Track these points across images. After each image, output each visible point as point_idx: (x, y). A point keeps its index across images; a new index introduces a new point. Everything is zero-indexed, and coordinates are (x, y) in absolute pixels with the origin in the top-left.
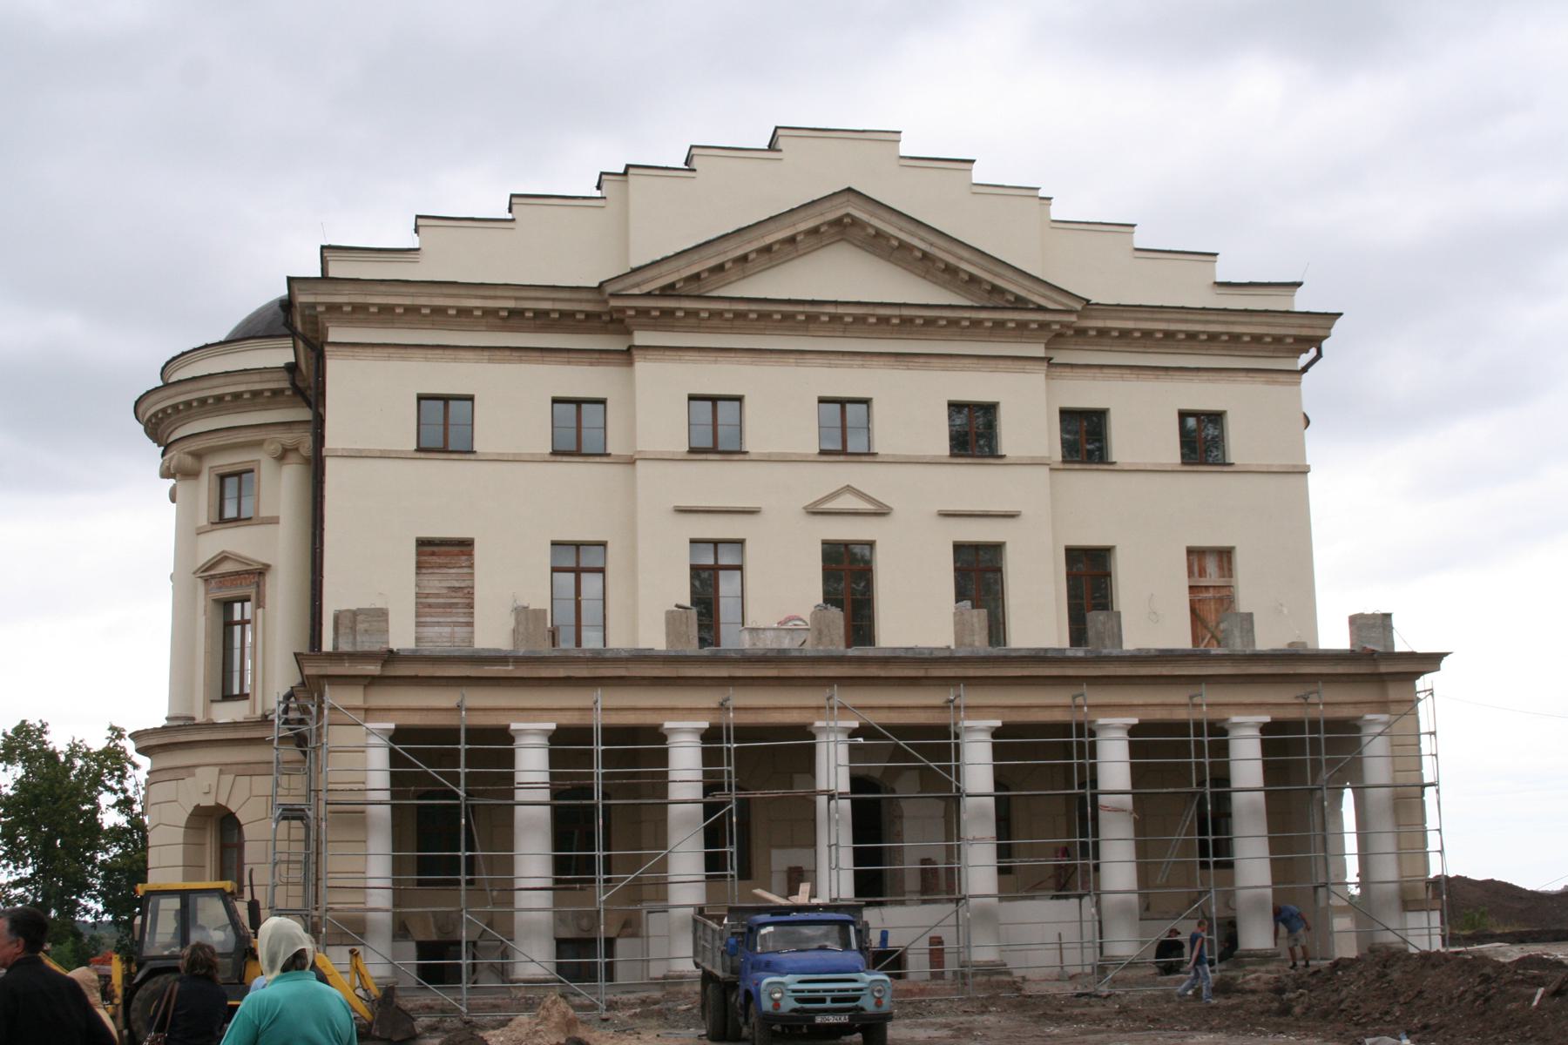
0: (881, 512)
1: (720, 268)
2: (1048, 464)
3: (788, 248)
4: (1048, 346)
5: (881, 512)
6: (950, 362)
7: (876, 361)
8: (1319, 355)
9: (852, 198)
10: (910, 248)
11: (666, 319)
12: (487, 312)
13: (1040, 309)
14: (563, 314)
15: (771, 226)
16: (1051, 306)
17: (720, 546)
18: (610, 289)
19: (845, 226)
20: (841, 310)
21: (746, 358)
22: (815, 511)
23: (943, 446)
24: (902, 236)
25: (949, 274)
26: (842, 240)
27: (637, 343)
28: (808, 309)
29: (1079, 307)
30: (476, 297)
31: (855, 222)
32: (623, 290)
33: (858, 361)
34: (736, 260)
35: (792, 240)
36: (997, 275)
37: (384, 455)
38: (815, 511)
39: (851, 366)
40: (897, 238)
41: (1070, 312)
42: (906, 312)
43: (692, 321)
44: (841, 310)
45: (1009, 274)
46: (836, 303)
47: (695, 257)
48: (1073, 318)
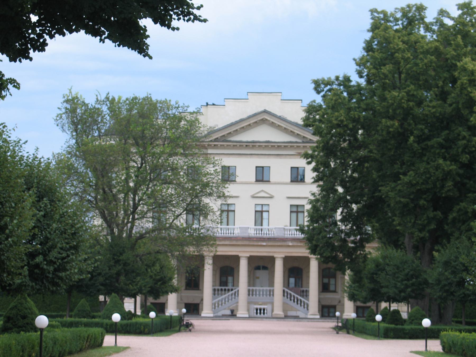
1: (230, 133)
5: (271, 197)
6: (291, 157)
7: (272, 157)
9: (265, 114)
10: (282, 127)
11: (215, 147)
20: (261, 144)
21: (237, 156)
23: (289, 180)
31: (266, 120)
33: (267, 157)
34: (234, 131)
35: (250, 125)
36: (304, 133)
38: (253, 197)
42: (279, 144)
44: (261, 144)
47: (223, 131)
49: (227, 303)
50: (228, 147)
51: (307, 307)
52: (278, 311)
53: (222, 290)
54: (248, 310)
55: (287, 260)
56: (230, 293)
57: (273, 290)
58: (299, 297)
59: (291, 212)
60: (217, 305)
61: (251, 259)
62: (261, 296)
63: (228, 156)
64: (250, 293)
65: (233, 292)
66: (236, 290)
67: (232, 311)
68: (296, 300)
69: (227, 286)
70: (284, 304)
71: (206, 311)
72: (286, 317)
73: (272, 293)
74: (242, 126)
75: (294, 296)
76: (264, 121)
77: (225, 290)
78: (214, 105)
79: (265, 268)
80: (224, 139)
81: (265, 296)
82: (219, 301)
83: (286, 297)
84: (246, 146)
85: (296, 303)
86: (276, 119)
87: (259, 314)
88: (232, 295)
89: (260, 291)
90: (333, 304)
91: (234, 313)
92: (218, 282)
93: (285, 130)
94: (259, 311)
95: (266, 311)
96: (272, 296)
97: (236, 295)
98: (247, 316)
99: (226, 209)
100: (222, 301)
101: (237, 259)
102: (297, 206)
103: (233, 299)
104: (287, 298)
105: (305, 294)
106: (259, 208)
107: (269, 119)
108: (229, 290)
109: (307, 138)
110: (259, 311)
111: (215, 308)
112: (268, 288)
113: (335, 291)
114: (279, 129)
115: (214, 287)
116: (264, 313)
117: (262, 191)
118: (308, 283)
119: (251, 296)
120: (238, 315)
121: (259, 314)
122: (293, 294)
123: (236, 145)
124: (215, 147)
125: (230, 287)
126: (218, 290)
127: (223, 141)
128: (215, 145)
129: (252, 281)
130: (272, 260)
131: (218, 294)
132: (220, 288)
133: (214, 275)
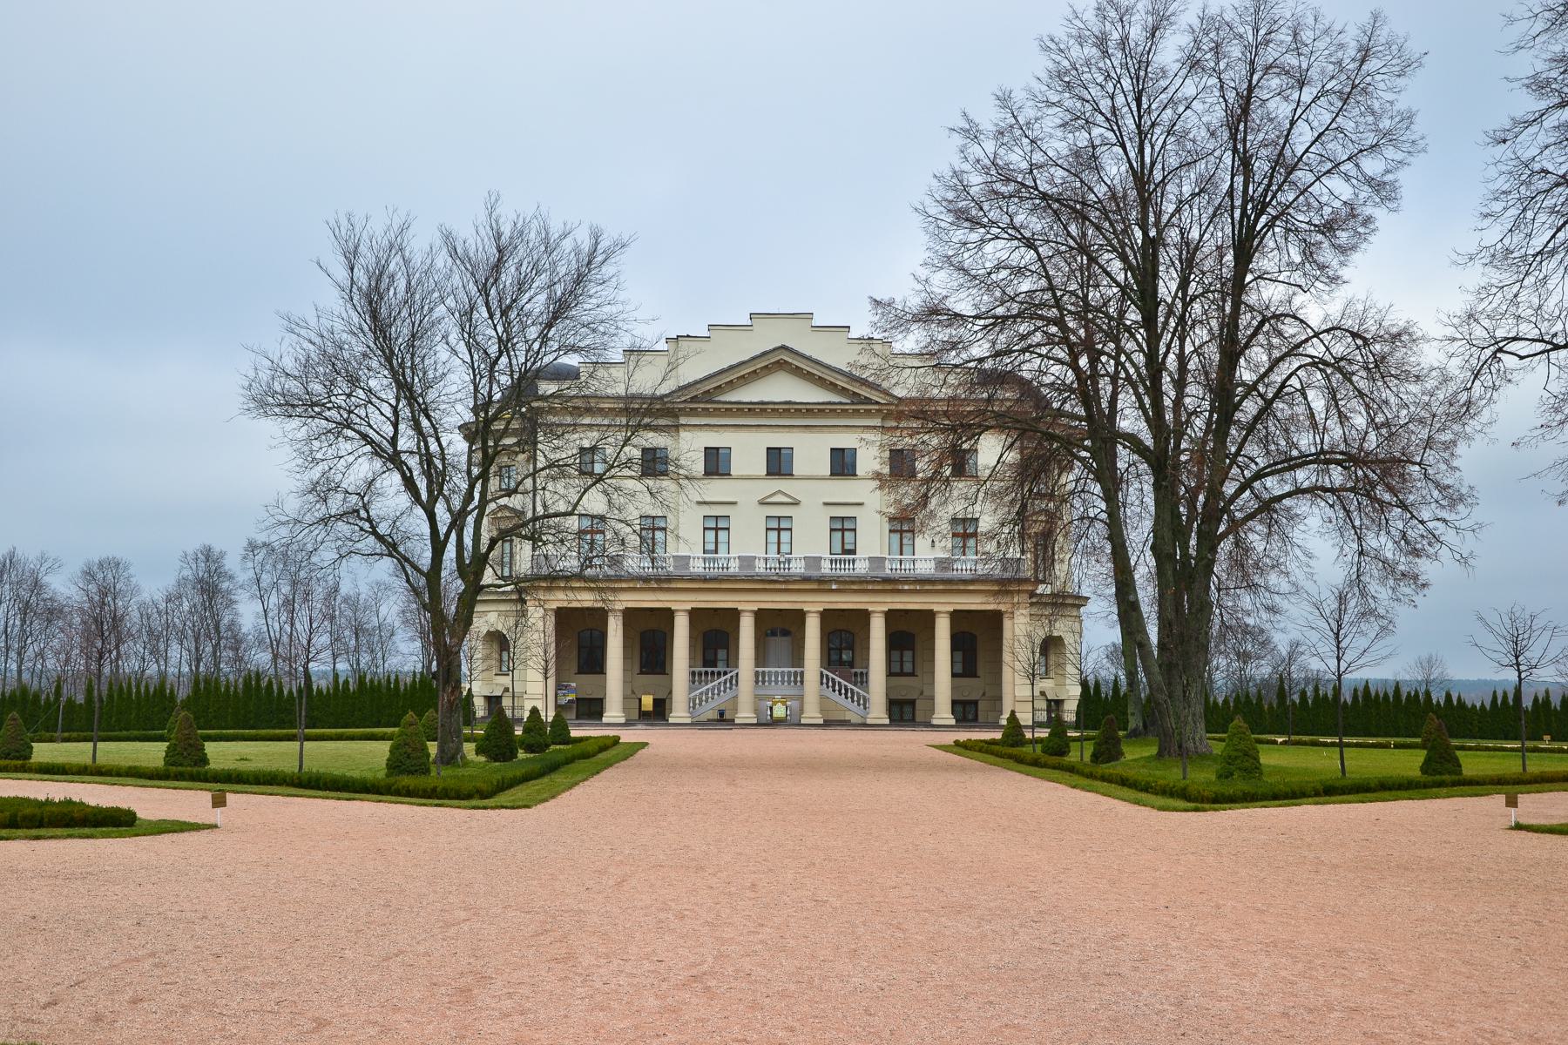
0: (796, 503)
3: (754, 375)
5: (796, 503)
6: (832, 429)
7: (795, 430)
11: (693, 412)
13: (877, 403)
15: (743, 366)
18: (666, 400)
22: (762, 503)
24: (808, 369)
28: (760, 406)
33: (787, 430)
38: (762, 503)
41: (892, 404)
42: (808, 407)
44: (776, 407)
46: (775, 403)
49: (716, 696)
50: (717, 413)
51: (865, 703)
52: (812, 714)
53: (706, 673)
55: (826, 616)
56: (723, 679)
57: (802, 674)
58: (850, 686)
59: (832, 530)
60: (697, 701)
61: (760, 616)
64: (759, 679)
65: (728, 676)
66: (734, 673)
68: (843, 691)
69: (716, 666)
70: (822, 697)
71: (679, 711)
72: (828, 724)
73: (799, 679)
74: (742, 373)
75: (840, 683)
76: (781, 366)
77: (713, 673)
78: (688, 336)
79: (785, 633)
80: (708, 396)
81: (786, 684)
82: (701, 693)
83: (825, 686)
84: (749, 409)
85: (843, 696)
86: (804, 361)
88: (725, 683)
89: (776, 673)
90: (973, 697)
91: (727, 716)
93: (821, 382)
96: (799, 684)
97: (734, 682)
98: (755, 721)
100: (707, 694)
101: (734, 615)
102: (843, 518)
103: (728, 690)
104: (828, 687)
105: (862, 679)
107: (790, 361)
108: (719, 673)
111: (694, 708)
112: (792, 670)
113: (913, 674)
118: (867, 659)
119: (760, 684)
120: (737, 721)
122: (837, 679)
123: (731, 409)
125: (722, 669)
126: (700, 674)
127: (707, 402)
129: (761, 658)
130: (800, 616)
131: (700, 683)
132: (703, 670)
133: (692, 646)
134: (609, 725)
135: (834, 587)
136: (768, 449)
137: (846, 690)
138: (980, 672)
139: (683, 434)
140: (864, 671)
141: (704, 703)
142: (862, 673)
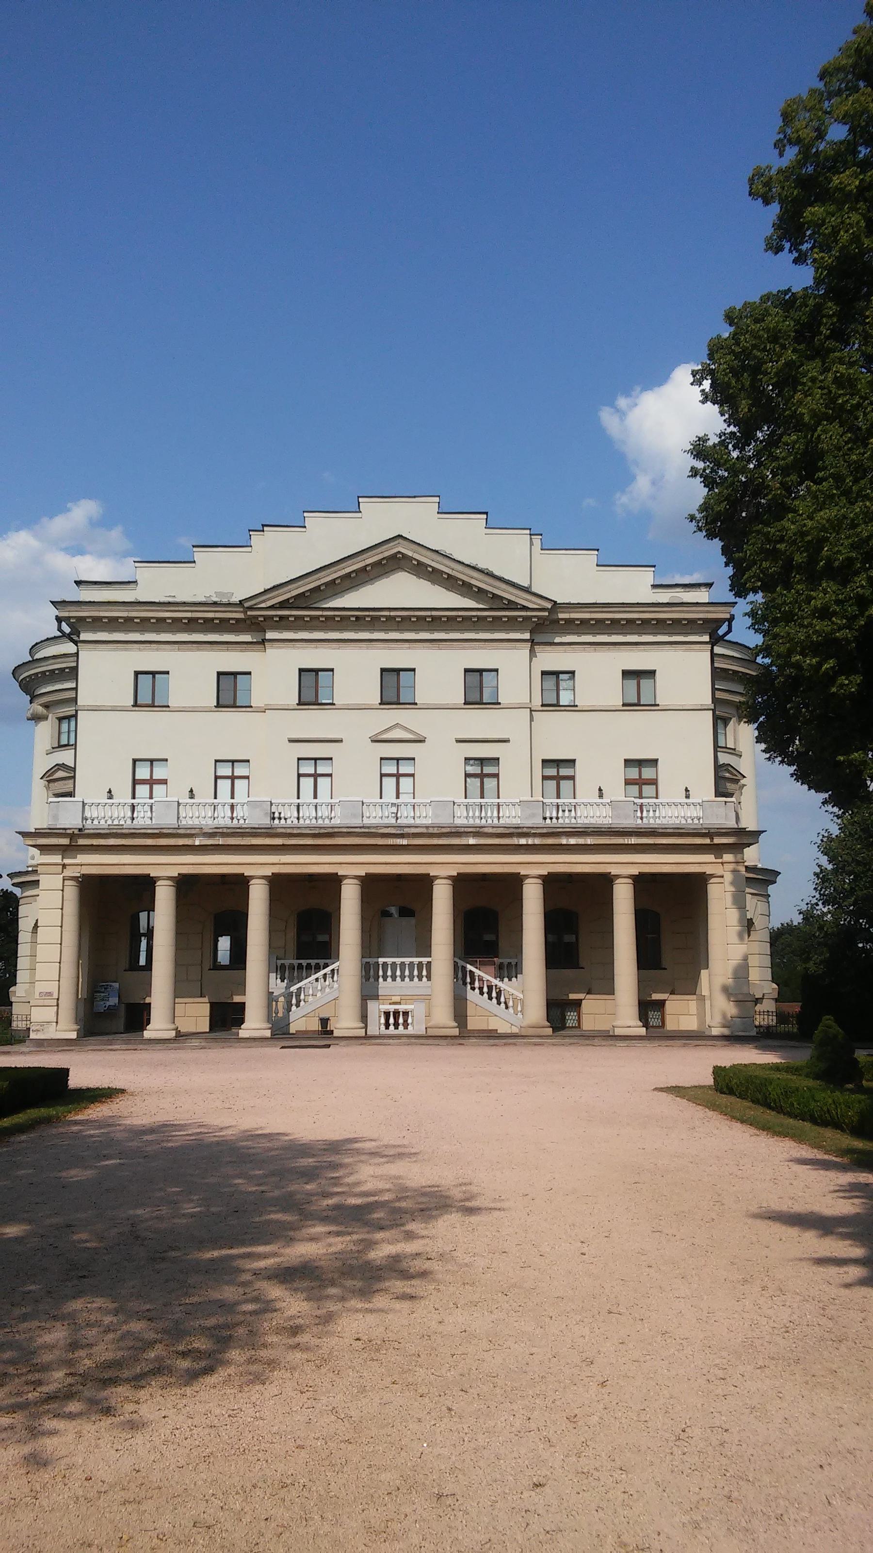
2: (530, 708)
4: (532, 632)
8: (730, 630)
9: (400, 541)
11: (282, 623)
12: (174, 620)
13: (525, 608)
14: (222, 620)
16: (531, 606)
17: (318, 761)
18: (246, 605)
19: (399, 559)
20: (392, 614)
25: (465, 588)
26: (399, 568)
27: (267, 638)
29: (549, 606)
30: (167, 611)
32: (255, 605)
35: (364, 569)
37: (114, 709)
39: (402, 648)
40: (431, 566)
42: (434, 613)
43: (301, 623)
44: (392, 614)
45: (503, 586)
48: (546, 614)
53: (300, 966)
54: (364, 1018)
56: (322, 972)
57: (429, 963)
58: (495, 982)
59: (467, 775)
62: (398, 979)
63: (314, 645)
65: (328, 970)
67: (324, 1022)
73: (424, 973)
79: (406, 912)
85: (486, 995)
86: (429, 553)
87: (392, 1027)
89: (394, 964)
92: (292, 947)
93: (450, 582)
94: (392, 1021)
95: (410, 1021)
98: (362, 1033)
99: (311, 771)
100: (298, 995)
101: (333, 882)
106: (391, 768)
107: (410, 554)
108: (318, 968)
109: (502, 598)
110: (392, 1021)
112: (416, 960)
114: (434, 582)
115: (280, 962)
116: (406, 1025)
117: (397, 725)
120: (336, 1034)
121: (392, 1027)
124: (283, 623)
126: (292, 967)
128: (281, 618)
132: (296, 962)
134: (151, 1041)
135: (472, 841)
136: (383, 670)
137: (490, 988)
138: (664, 964)
139: (272, 653)
140: (513, 961)
141: (294, 1008)
142: (510, 963)
